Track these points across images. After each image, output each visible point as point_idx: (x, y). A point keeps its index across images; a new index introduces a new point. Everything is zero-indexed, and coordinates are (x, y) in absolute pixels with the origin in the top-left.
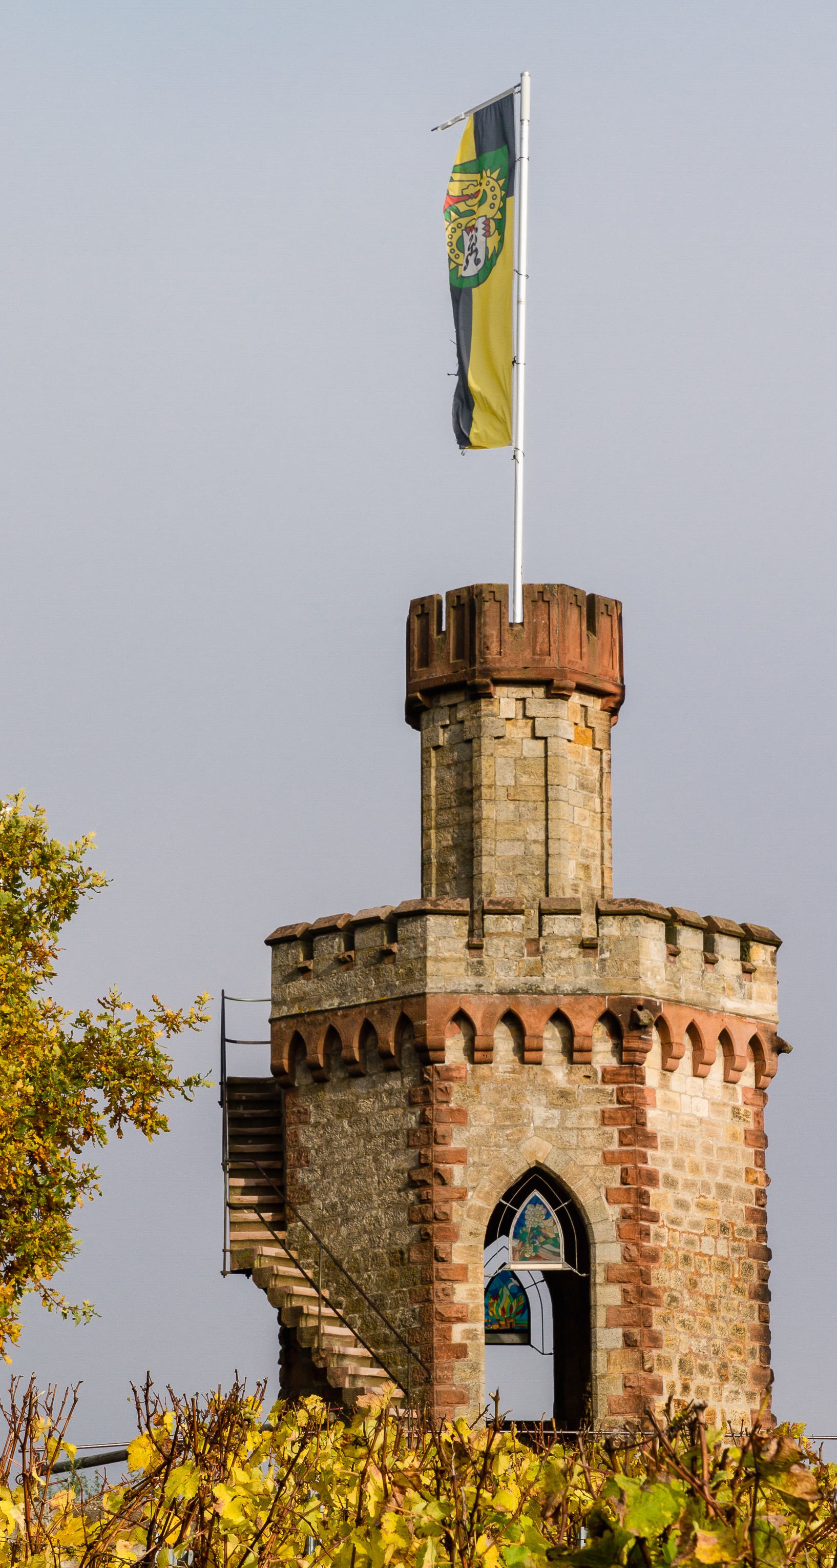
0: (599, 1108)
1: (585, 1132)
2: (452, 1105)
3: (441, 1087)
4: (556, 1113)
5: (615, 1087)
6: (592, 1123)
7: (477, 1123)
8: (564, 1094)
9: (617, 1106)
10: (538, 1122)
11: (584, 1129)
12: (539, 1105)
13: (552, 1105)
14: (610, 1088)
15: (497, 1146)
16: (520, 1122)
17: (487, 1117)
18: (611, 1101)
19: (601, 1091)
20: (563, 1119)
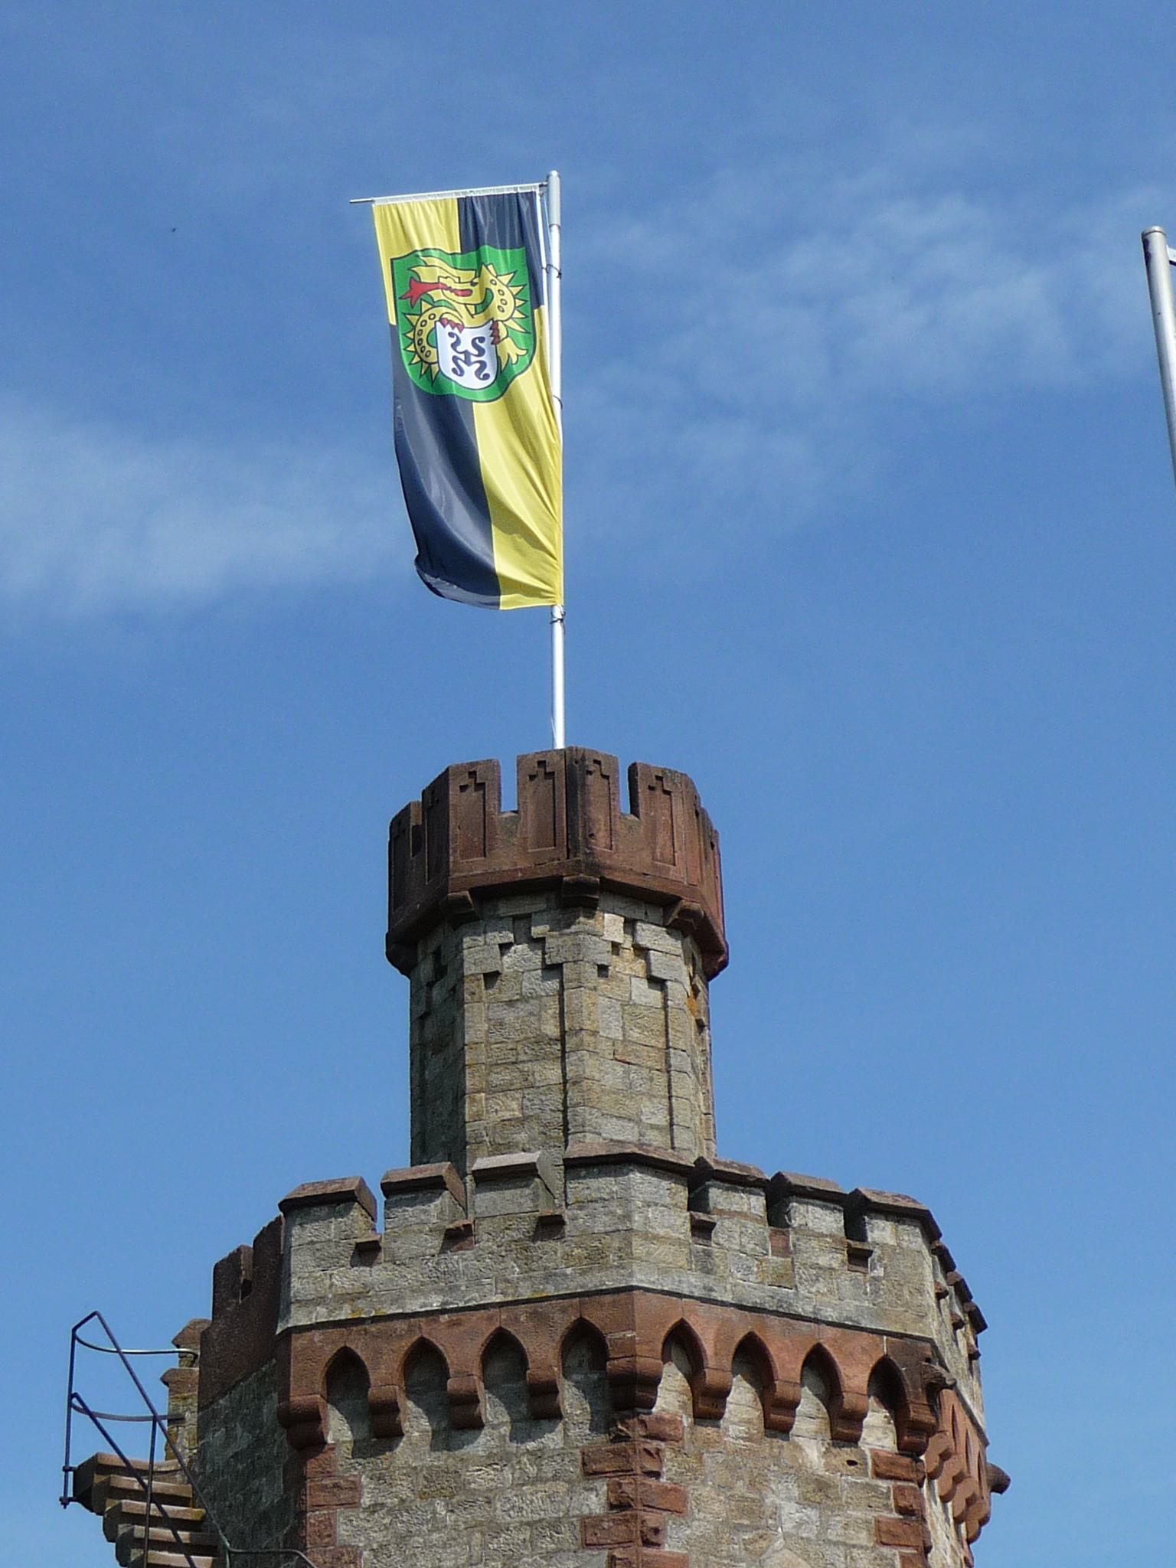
0: (871, 1515)
1: (855, 1552)
2: (663, 1480)
3: (648, 1446)
4: (812, 1514)
5: (890, 1484)
6: (863, 1538)
7: (702, 1515)
8: (822, 1486)
9: (895, 1515)
10: (788, 1526)
11: (854, 1546)
12: (789, 1499)
13: (805, 1501)
14: (883, 1484)
15: (731, 1557)
16: (763, 1522)
17: (716, 1507)
18: (886, 1506)
19: (875, 1488)
20: (824, 1526)
